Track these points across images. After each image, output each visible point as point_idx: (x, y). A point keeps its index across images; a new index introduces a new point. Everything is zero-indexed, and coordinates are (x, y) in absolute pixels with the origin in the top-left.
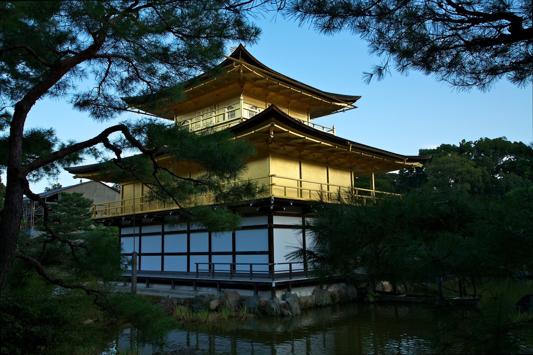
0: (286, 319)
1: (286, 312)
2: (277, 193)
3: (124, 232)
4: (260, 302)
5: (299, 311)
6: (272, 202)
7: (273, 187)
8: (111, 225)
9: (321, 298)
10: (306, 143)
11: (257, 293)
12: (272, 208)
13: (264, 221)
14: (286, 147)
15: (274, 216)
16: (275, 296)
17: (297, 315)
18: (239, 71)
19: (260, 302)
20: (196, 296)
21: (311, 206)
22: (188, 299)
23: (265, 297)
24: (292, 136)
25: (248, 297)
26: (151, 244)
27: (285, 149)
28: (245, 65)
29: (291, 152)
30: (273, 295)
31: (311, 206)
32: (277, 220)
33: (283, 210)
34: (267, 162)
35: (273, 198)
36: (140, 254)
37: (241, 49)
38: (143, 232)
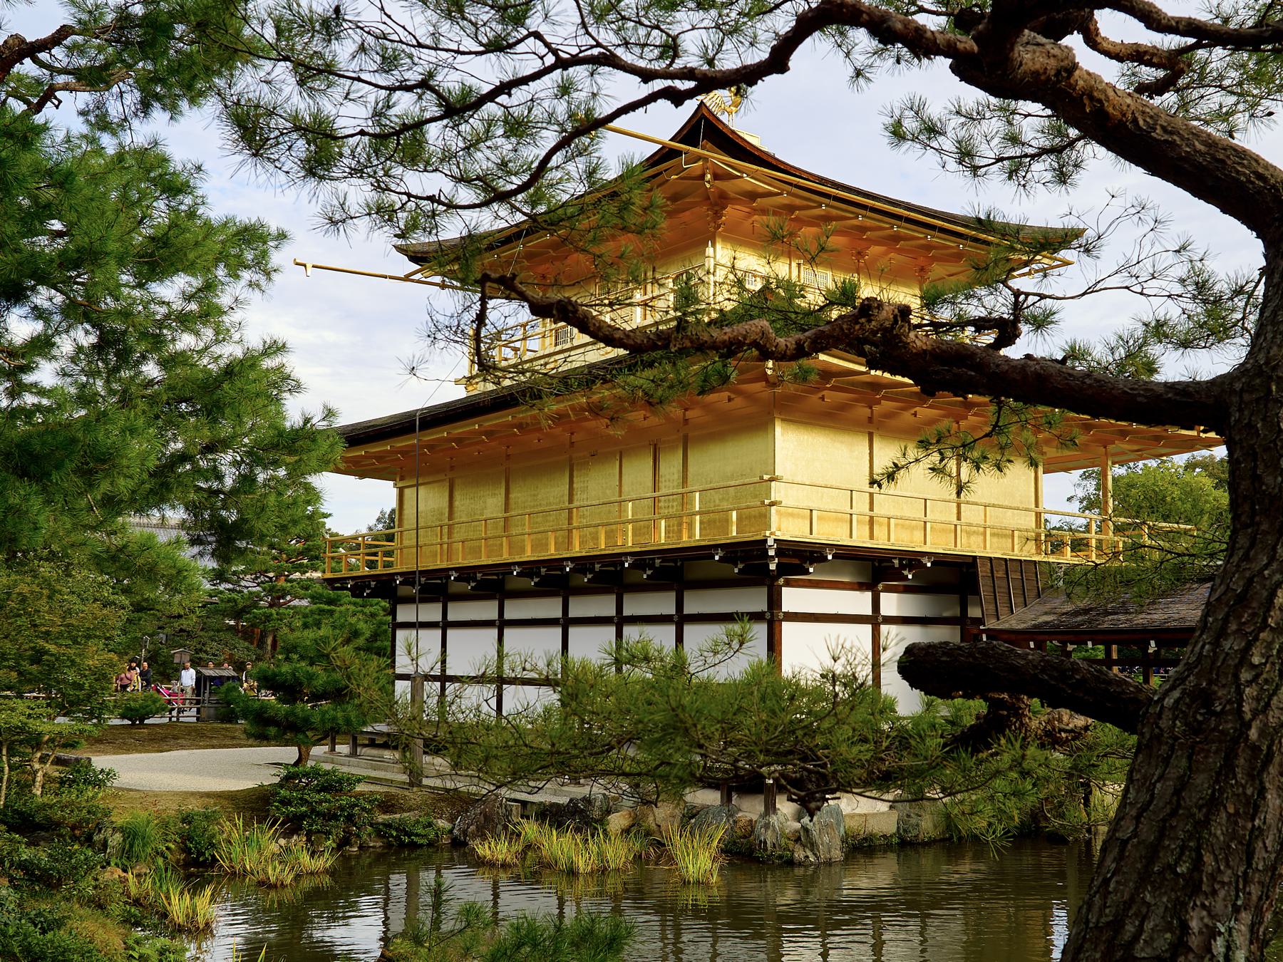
0: (799, 871)
1: (799, 854)
2: (785, 528)
3: (405, 613)
4: (735, 822)
5: (837, 854)
6: (771, 553)
7: (773, 509)
8: (369, 596)
9: (913, 821)
10: (876, 386)
11: (729, 800)
12: (773, 567)
13: (755, 600)
14: (825, 393)
15: (784, 589)
16: (775, 810)
17: (829, 863)
18: (702, 177)
19: (735, 822)
20: (571, 800)
21: (896, 562)
22: (553, 805)
23: (750, 809)
24: (834, 369)
25: (706, 808)
26: (471, 651)
27: (823, 398)
28: (720, 159)
29: (843, 407)
30: (770, 808)
31: (896, 562)
32: (793, 599)
33: (807, 573)
34: (770, 436)
35: (770, 542)
36: (444, 679)
37: (703, 116)
38: (451, 618)
